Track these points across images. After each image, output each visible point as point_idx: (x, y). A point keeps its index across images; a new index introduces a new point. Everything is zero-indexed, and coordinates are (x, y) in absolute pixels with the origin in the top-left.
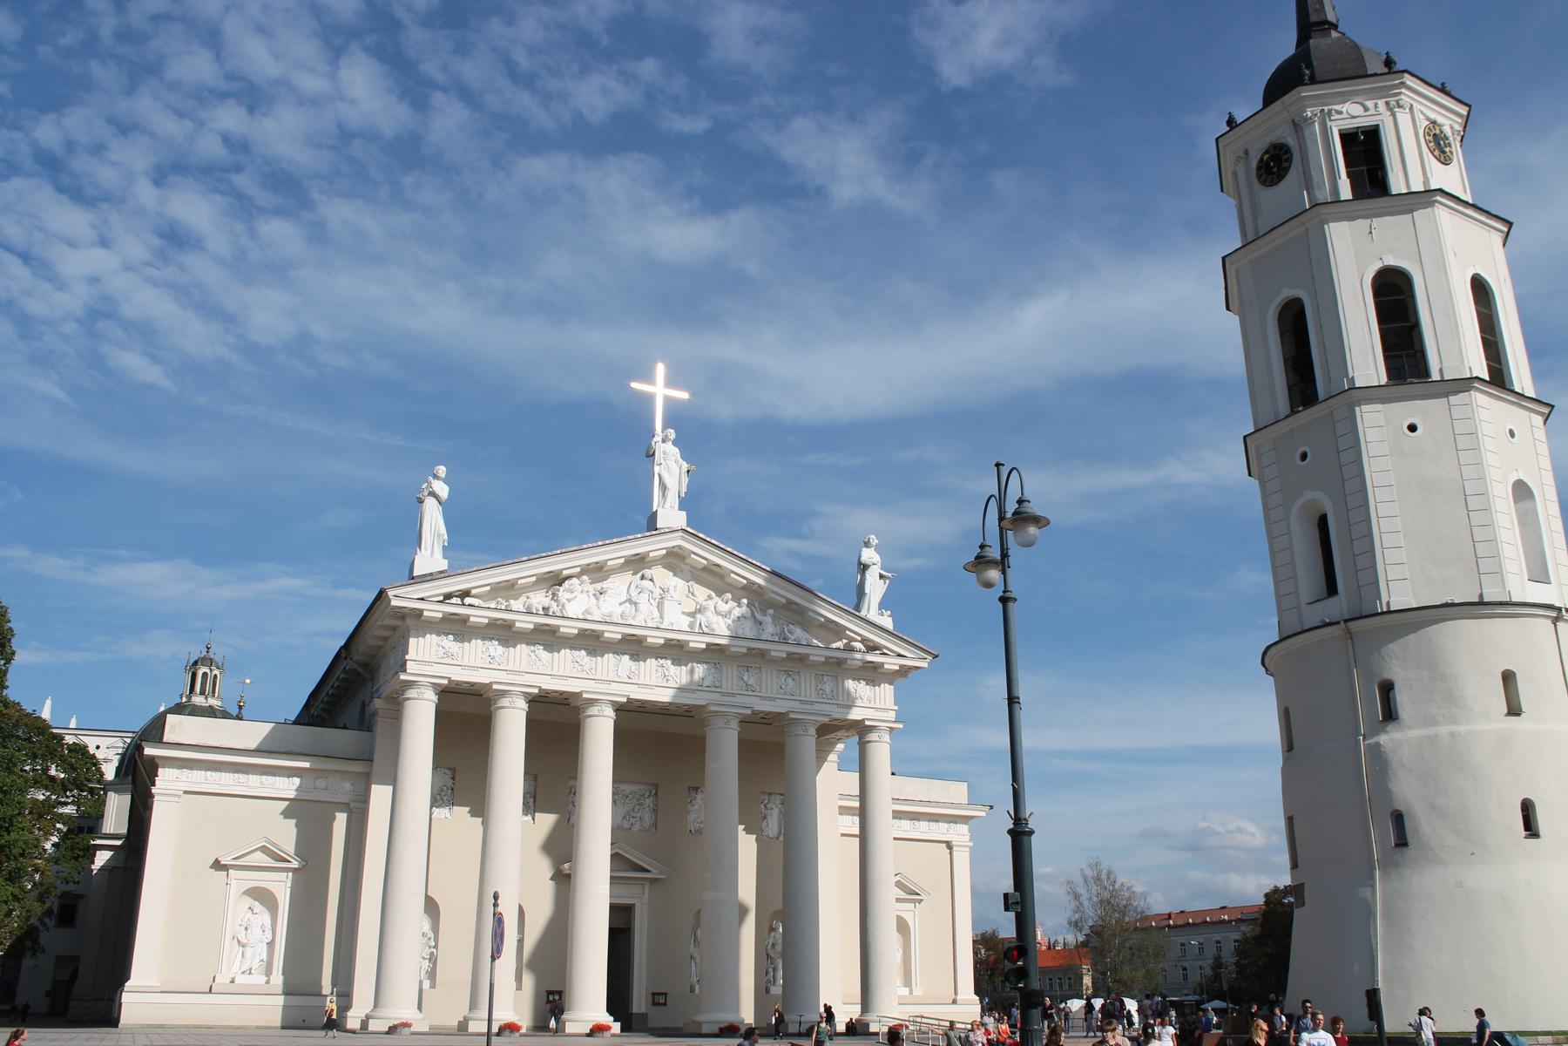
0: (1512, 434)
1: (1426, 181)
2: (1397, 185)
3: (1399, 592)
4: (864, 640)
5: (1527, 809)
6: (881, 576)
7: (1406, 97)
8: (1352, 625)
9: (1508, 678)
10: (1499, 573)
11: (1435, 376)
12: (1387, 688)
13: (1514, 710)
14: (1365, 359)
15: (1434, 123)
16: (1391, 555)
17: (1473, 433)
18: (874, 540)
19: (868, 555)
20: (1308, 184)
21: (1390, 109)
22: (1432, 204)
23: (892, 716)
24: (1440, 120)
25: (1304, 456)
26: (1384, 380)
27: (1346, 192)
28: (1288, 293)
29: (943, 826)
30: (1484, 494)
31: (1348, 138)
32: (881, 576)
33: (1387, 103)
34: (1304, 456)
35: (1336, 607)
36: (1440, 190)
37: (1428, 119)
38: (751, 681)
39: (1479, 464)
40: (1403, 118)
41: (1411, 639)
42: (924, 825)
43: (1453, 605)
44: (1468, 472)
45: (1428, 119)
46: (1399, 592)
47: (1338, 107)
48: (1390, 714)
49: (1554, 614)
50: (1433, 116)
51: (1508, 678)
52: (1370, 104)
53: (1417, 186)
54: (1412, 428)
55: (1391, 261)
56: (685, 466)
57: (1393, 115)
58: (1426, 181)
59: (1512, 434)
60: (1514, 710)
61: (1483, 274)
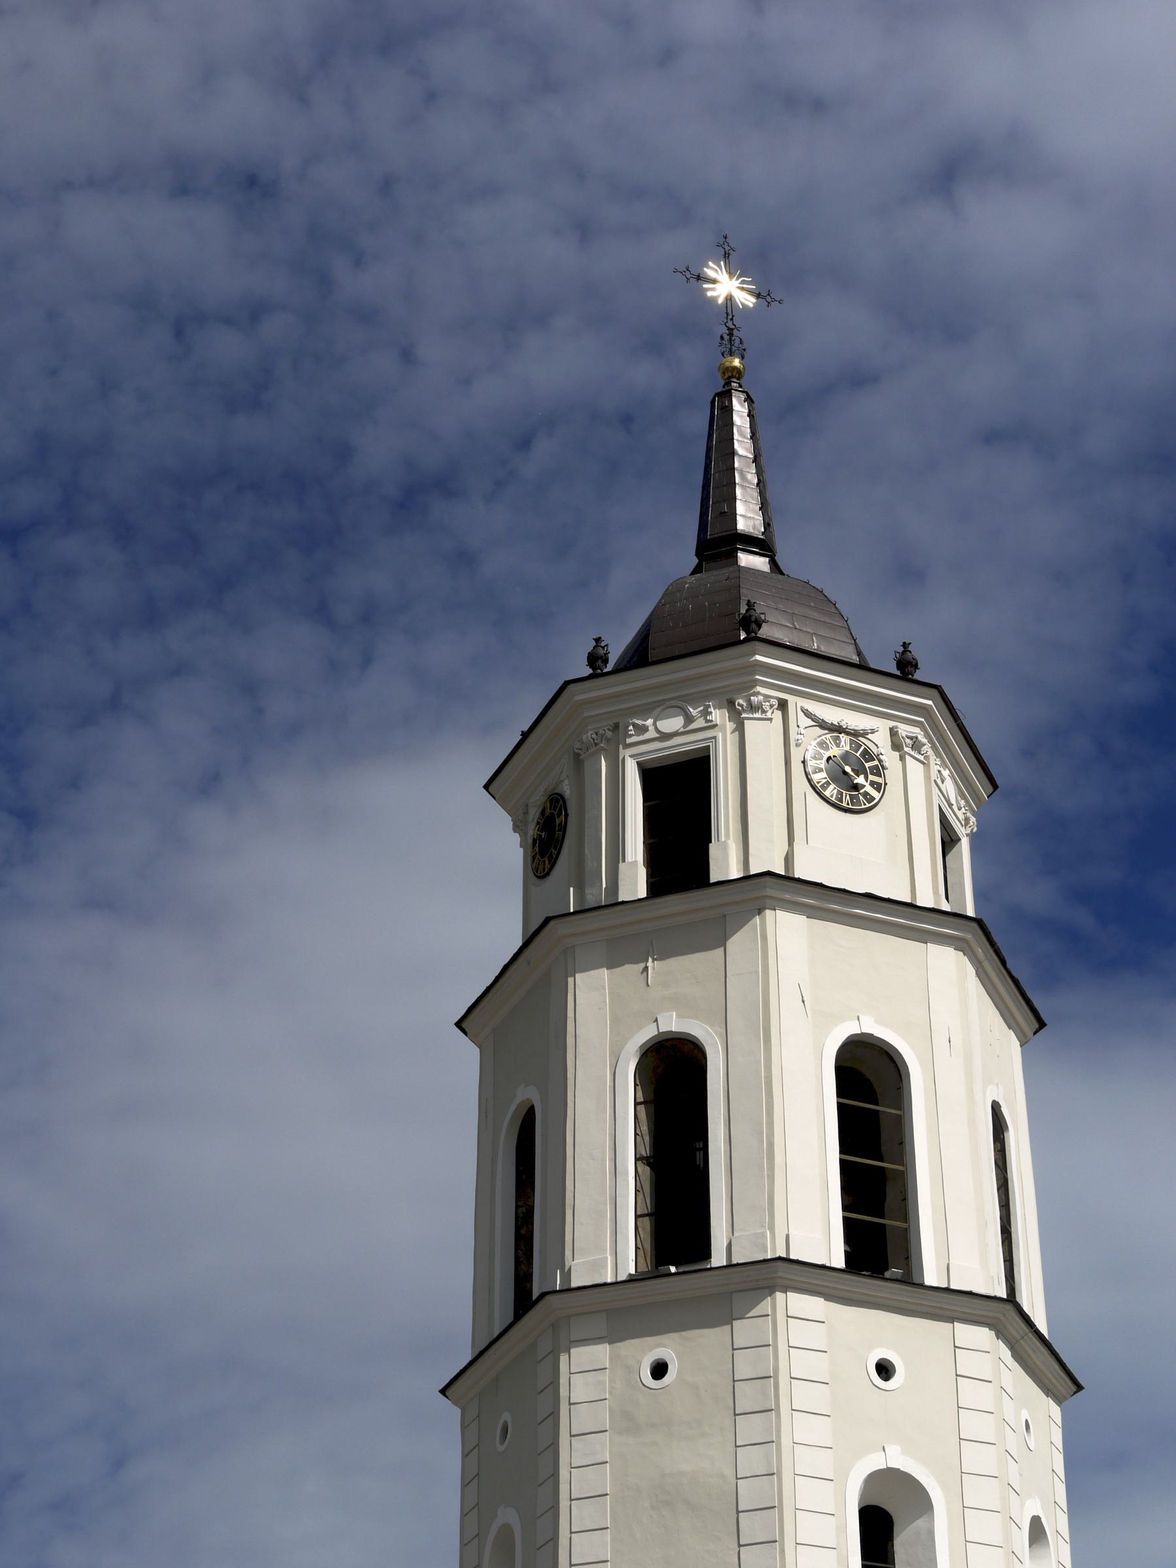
0: (885, 1370)
1: (789, 860)
7: (764, 692)
11: (718, 1258)
14: (602, 1230)
15: (838, 729)
17: (768, 1378)
31: (655, 778)
37: (822, 725)
39: (770, 1442)
40: (763, 734)
44: (750, 1460)
45: (822, 725)
54: (659, 1370)
58: (789, 860)
59: (885, 1370)
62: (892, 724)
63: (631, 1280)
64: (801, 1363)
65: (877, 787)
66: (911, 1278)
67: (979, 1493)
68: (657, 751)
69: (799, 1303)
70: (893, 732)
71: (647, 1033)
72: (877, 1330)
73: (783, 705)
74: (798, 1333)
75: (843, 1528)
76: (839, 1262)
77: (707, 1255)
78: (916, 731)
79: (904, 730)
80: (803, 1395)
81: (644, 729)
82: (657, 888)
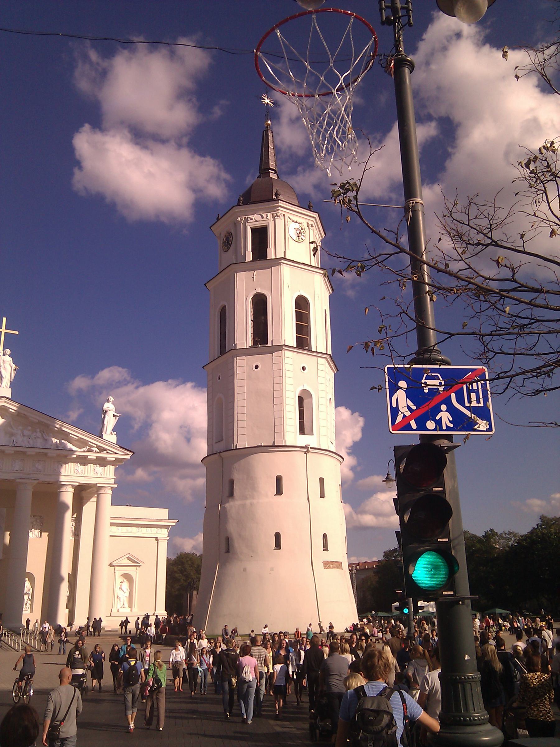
0: (304, 369)
2: (271, 255)
3: (242, 440)
4: (98, 447)
5: (278, 536)
6: (114, 416)
8: (221, 454)
10: (283, 432)
11: (270, 344)
12: (232, 482)
13: (279, 492)
14: (243, 335)
16: (240, 424)
17: (281, 370)
18: (111, 399)
19: (107, 406)
20: (236, 252)
21: (273, 217)
22: (280, 264)
23: (113, 481)
24: (299, 220)
27: (249, 257)
29: (154, 530)
30: (281, 397)
32: (114, 416)
38: (40, 467)
39: (281, 383)
40: (280, 222)
41: (242, 462)
42: (144, 529)
43: (261, 446)
44: (276, 387)
46: (242, 440)
47: (250, 216)
48: (231, 494)
49: (305, 450)
51: (279, 480)
52: (264, 215)
53: (280, 255)
54: (257, 367)
56: (14, 366)
57: (274, 220)
58: (285, 253)
59: (304, 369)
60: (279, 492)
62: (308, 221)
63: (250, 347)
64: (287, 367)
66: (310, 350)
67: (321, 394)
69: (287, 354)
70: (308, 223)
71: (254, 292)
72: (302, 358)
73: (284, 215)
74: (287, 361)
75: (295, 401)
76: (295, 345)
78: (312, 223)
79: (310, 223)
80: (288, 374)
81: (252, 219)
82: (254, 259)
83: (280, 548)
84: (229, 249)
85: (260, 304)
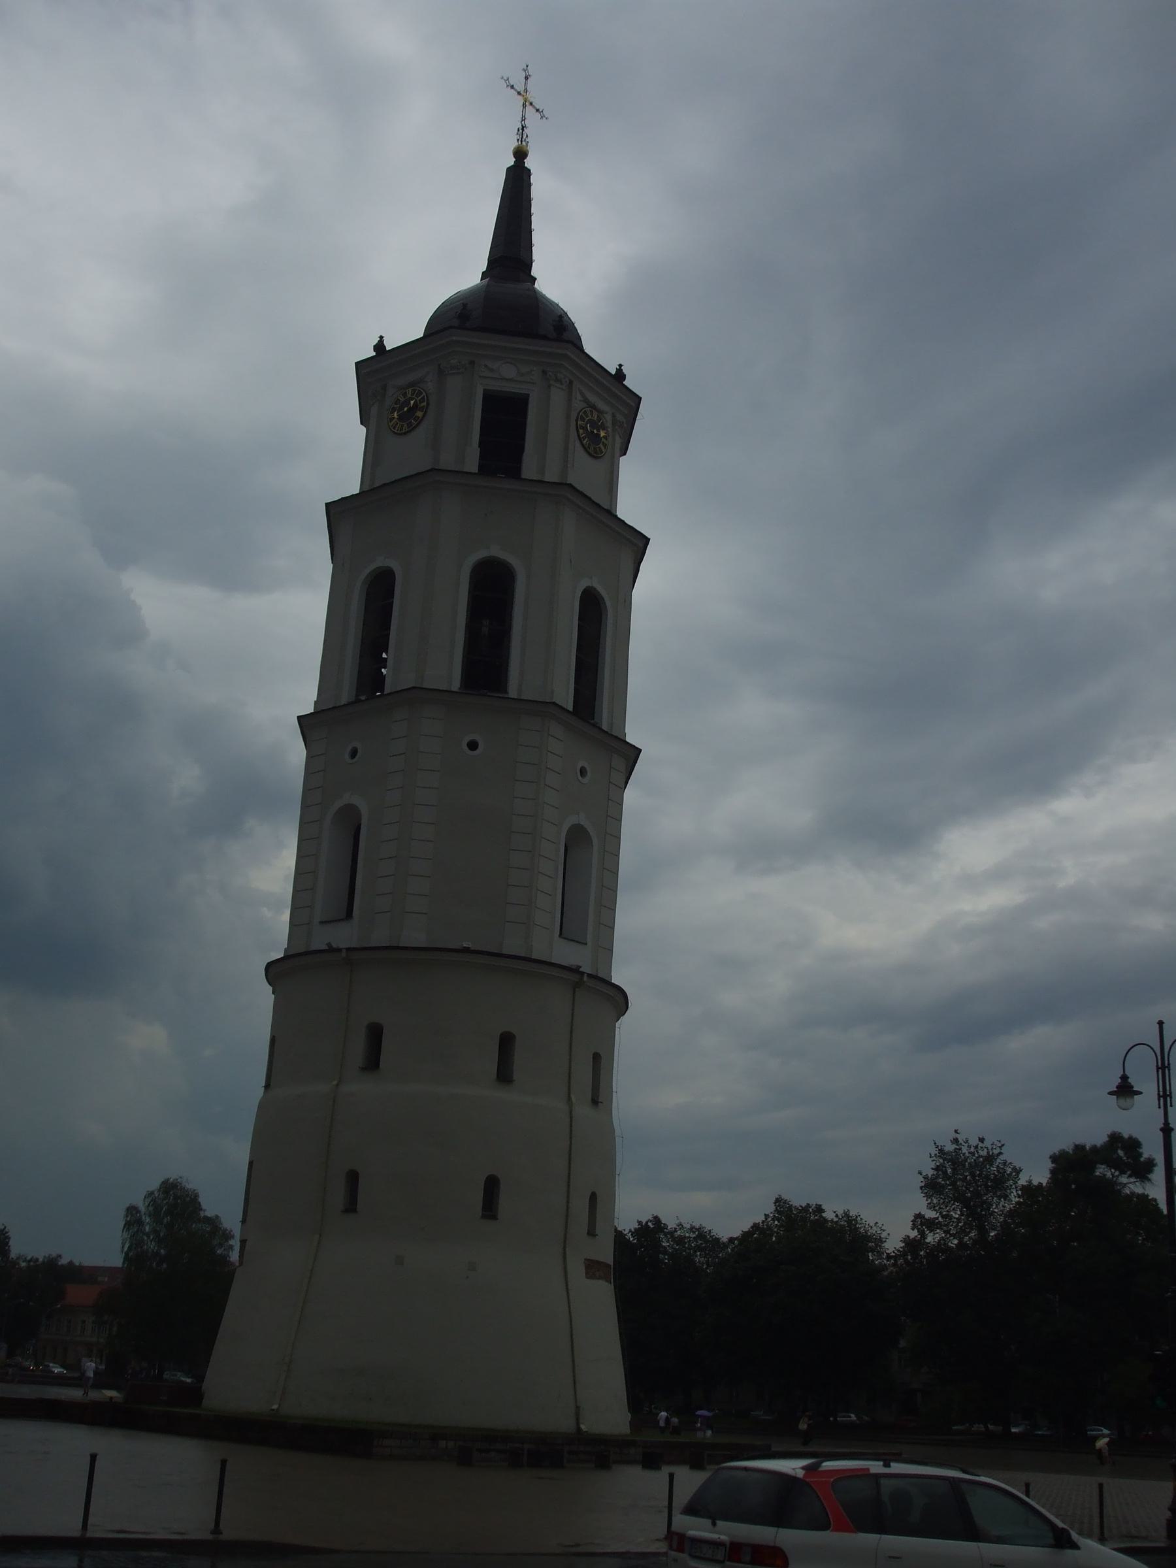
0: (583, 772)
2: (529, 470)
5: (492, 1186)
9: (506, 1041)
12: (375, 1034)
13: (504, 1076)
15: (593, 407)
24: (601, 405)
25: (354, 753)
26: (456, 685)
28: (380, 562)
31: (493, 401)
33: (544, 372)
34: (354, 753)
35: (344, 936)
36: (570, 485)
37: (586, 400)
40: (558, 396)
43: (466, 950)
45: (586, 400)
48: (372, 1063)
50: (593, 399)
51: (506, 1041)
53: (551, 476)
54: (473, 746)
55: (496, 551)
59: (583, 772)
60: (504, 1076)
61: (600, 589)
65: (605, 446)
68: (495, 386)
70: (614, 416)
73: (571, 382)
76: (571, 708)
77: (506, 692)
83: (494, 1217)
84: (412, 429)
85: (492, 590)
